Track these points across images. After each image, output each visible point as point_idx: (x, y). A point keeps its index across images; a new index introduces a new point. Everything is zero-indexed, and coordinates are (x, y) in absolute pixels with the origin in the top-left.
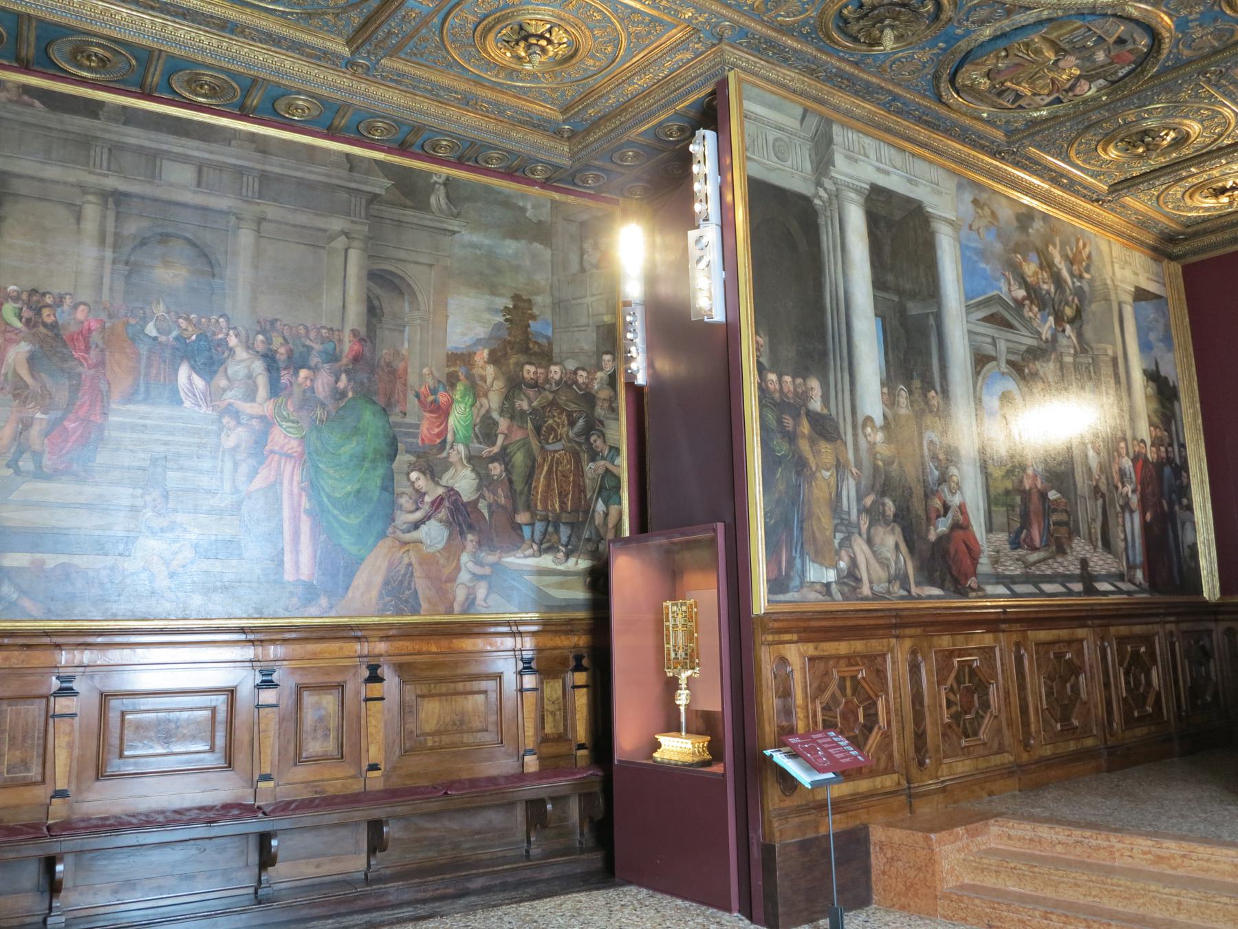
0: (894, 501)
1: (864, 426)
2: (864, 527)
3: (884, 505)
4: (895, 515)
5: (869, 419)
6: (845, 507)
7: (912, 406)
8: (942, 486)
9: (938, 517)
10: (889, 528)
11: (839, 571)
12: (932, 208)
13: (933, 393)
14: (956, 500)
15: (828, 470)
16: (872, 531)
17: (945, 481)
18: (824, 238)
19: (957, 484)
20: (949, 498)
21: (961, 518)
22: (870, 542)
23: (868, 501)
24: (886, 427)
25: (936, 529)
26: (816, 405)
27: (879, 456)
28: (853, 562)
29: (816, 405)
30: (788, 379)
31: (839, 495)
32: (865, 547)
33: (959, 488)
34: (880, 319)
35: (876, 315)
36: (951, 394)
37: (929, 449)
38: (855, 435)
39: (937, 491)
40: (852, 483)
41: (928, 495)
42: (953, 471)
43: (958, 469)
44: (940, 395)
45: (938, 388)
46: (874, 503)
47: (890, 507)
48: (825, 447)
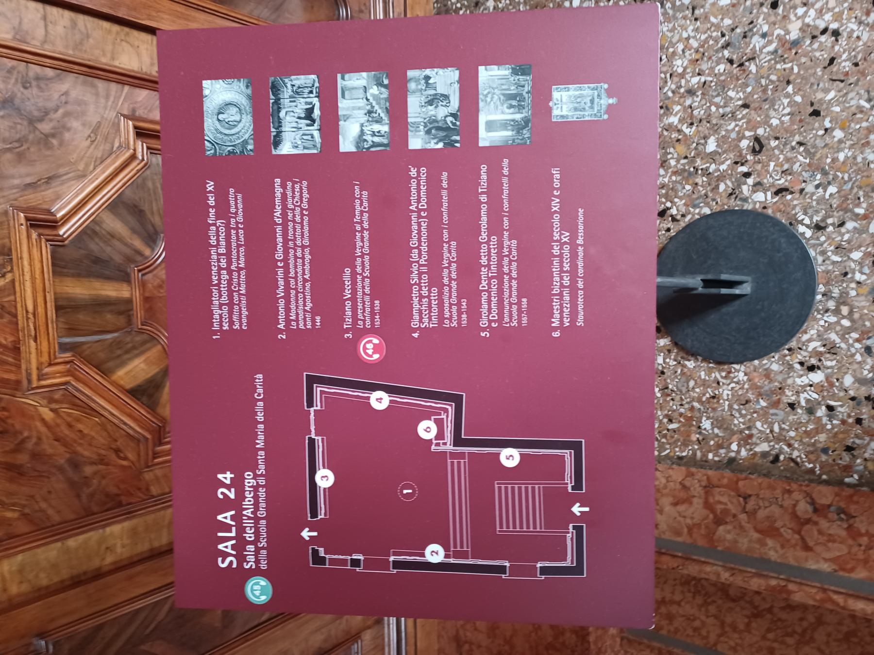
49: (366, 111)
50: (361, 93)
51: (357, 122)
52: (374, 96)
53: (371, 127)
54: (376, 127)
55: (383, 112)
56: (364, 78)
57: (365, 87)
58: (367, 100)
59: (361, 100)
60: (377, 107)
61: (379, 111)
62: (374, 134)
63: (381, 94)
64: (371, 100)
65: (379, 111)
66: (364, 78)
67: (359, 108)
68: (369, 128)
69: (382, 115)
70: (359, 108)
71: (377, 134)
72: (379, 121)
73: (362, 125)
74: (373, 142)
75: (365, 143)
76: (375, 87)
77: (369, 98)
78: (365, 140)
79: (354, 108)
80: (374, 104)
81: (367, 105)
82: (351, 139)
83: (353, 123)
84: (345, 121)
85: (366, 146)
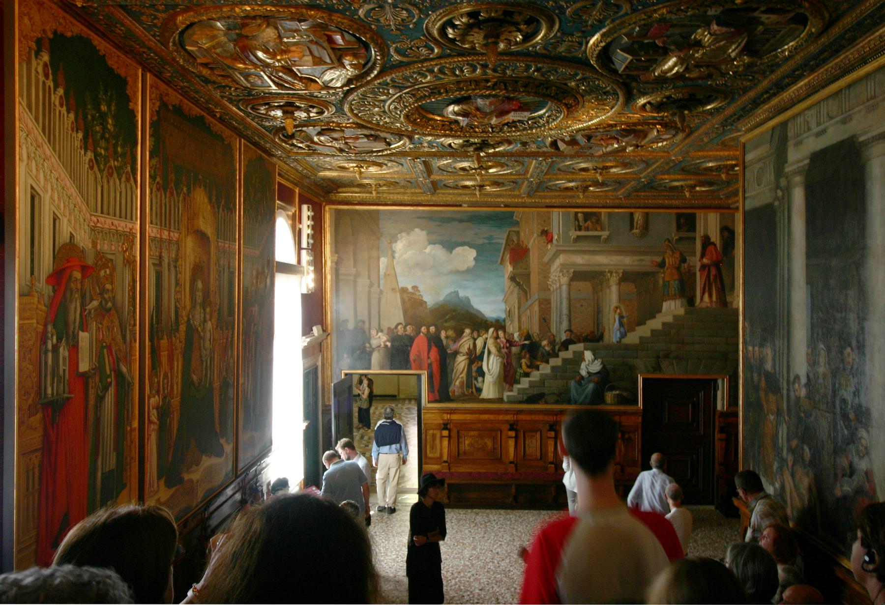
0: (810, 449)
1: (794, 383)
2: (790, 464)
3: (803, 450)
4: (810, 461)
5: (797, 377)
6: (780, 446)
7: (829, 364)
8: (851, 446)
9: (844, 475)
10: (805, 471)
11: (775, 489)
12: (865, 133)
13: (848, 350)
14: (862, 465)
15: (772, 414)
16: (795, 468)
17: (854, 442)
18: (779, 232)
19: (866, 448)
20: (856, 460)
21: (867, 485)
22: (793, 476)
23: (794, 443)
24: (808, 384)
25: (841, 486)
26: (768, 366)
27: (802, 409)
28: (783, 487)
29: (768, 366)
30: (757, 349)
31: (777, 435)
32: (790, 479)
33: (868, 453)
34: (809, 286)
35: (807, 283)
36: (867, 350)
37: (841, 408)
38: (788, 390)
39: (845, 450)
40: (785, 426)
41: (837, 451)
42: (862, 433)
43: (868, 432)
44: (856, 351)
45: (854, 343)
46: (797, 446)
47: (807, 453)
48: (772, 398)
49: (536, 338)
50: (584, 325)
51: (509, 313)
52: (579, 358)
53: (493, 350)
54: (492, 365)
55: (532, 385)
56: (623, 336)
57: (601, 338)
58: (565, 345)
59: (565, 325)
60: (545, 369)
61: (535, 376)
62: (475, 358)
63: (580, 384)
64: (563, 355)
65: (535, 376)
66: (623, 336)
67: (545, 321)
68: (490, 343)
69: (525, 383)
70: (545, 321)
71: (474, 368)
72: (508, 377)
73: (499, 325)
74: (456, 353)
75: (451, 333)
76: (596, 367)
77: (572, 348)
78: (460, 334)
79: (545, 305)
80: (555, 362)
81: (552, 343)
82: (462, 294)
83: (505, 301)
84: (513, 279)
85: (443, 334)
